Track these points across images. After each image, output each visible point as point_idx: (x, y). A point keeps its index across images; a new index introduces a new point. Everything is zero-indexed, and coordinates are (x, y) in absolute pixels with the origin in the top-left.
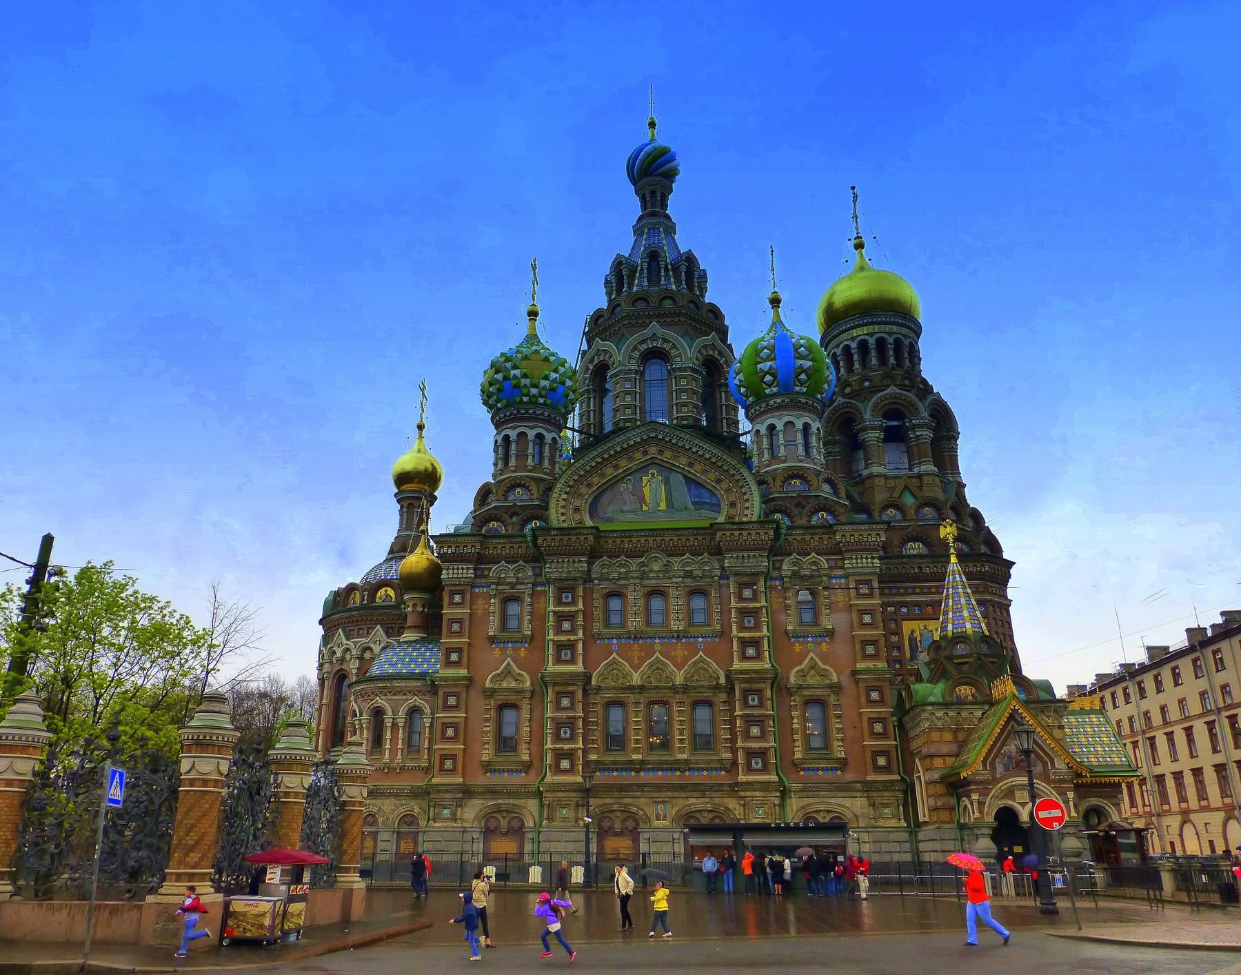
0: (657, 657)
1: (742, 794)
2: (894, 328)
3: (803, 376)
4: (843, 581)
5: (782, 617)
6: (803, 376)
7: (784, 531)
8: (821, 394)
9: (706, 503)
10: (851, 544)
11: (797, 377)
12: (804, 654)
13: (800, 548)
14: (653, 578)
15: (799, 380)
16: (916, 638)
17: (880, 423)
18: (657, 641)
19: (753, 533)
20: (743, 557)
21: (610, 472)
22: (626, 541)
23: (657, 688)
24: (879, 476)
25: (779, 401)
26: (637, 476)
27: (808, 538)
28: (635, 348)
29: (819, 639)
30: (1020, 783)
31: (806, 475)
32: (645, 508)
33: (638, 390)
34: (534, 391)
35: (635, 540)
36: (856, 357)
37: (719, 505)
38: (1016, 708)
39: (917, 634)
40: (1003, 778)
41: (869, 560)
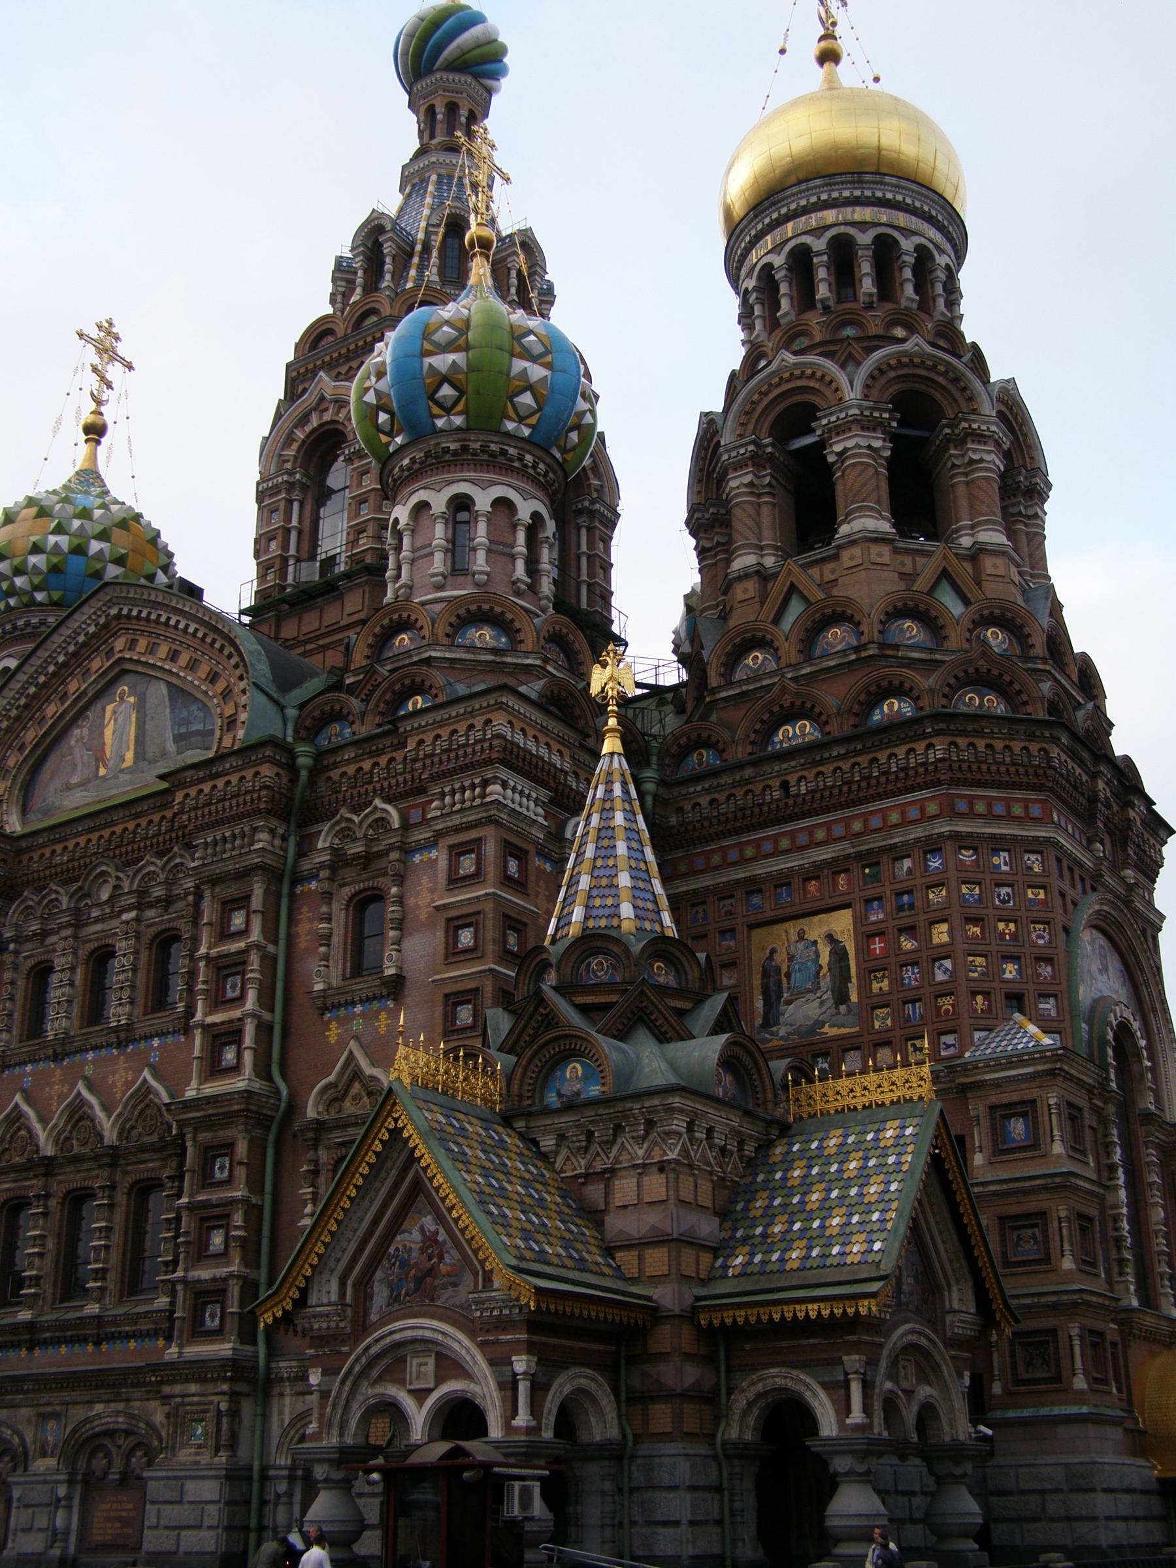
0: (79, 1094)
1: (167, 1390)
2: (830, 216)
3: (446, 390)
4: (434, 854)
5: (314, 965)
6: (446, 390)
7: (302, 761)
8: (521, 419)
9: (197, 733)
10: (436, 760)
11: (431, 397)
12: (342, 1043)
13: (355, 792)
14: (97, 920)
15: (440, 405)
16: (778, 969)
17: (751, 448)
18: (90, 1056)
19: (234, 778)
20: (225, 840)
21: (52, 710)
22: (59, 848)
23: (77, 1159)
24: (744, 576)
25: (406, 462)
26: (99, 706)
27: (367, 765)
28: (290, 439)
29: (375, 1005)
30: (409, 1334)
31: (413, 618)
32: (102, 771)
33: (295, 522)
34: (19, 581)
35: (71, 844)
36: (757, 310)
37: (212, 732)
38: (400, 1124)
39: (781, 958)
40: (385, 1320)
41: (478, 790)
